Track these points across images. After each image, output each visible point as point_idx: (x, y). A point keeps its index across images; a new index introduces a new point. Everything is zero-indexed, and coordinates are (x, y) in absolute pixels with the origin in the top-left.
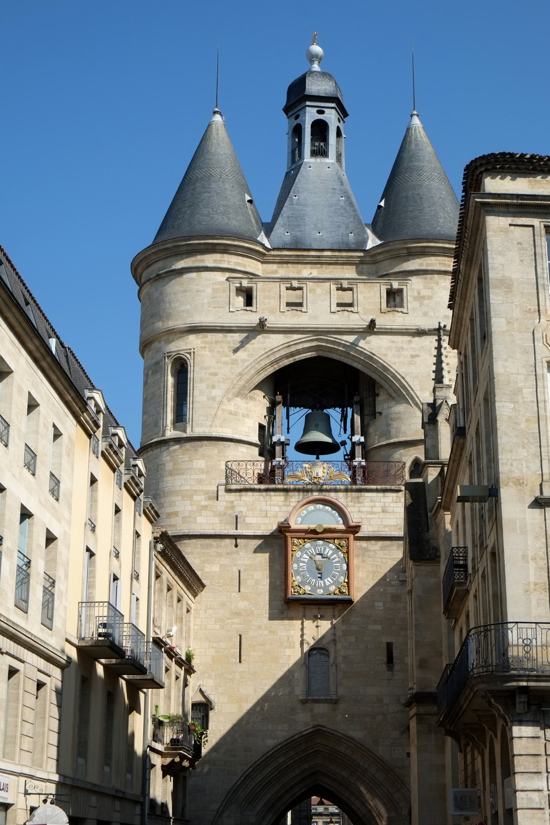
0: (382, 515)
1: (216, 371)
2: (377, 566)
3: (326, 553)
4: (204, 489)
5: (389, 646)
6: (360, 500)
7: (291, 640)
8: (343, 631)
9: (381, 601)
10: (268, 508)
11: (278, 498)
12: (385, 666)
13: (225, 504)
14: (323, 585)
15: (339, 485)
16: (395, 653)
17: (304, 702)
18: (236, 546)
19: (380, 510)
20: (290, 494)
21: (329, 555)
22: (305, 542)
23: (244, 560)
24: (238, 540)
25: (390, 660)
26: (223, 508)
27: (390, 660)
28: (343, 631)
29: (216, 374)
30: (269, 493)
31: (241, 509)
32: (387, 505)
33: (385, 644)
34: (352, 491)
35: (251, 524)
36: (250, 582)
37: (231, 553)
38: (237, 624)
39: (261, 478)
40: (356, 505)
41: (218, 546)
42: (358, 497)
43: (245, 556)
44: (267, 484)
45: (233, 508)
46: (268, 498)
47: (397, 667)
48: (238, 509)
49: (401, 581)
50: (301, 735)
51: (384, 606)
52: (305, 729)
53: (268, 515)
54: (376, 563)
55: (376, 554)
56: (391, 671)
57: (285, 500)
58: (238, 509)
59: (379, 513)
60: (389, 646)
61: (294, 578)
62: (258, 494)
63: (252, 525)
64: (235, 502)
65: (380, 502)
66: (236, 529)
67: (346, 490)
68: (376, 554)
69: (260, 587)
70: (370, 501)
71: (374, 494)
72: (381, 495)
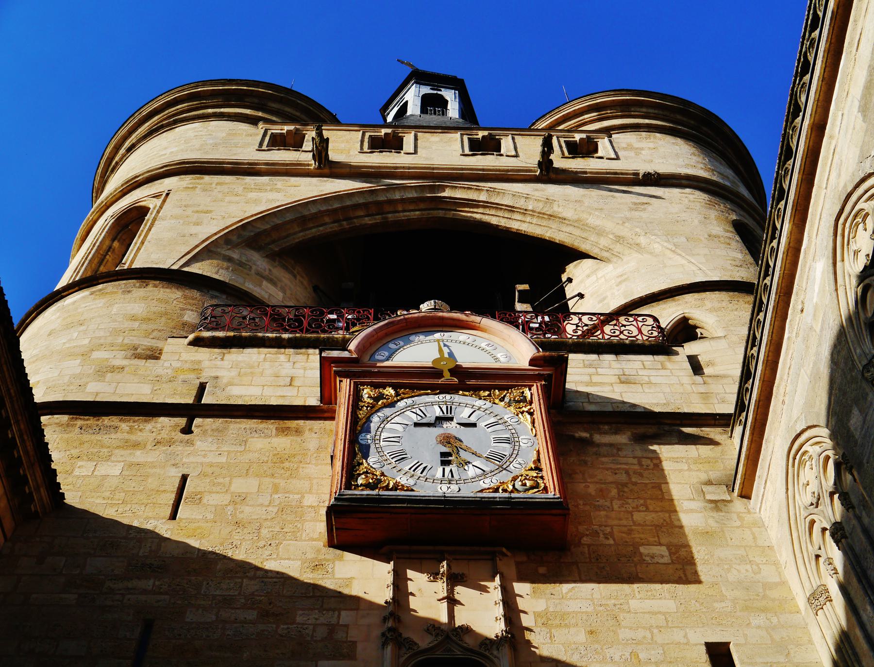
1: (209, 208)
4: (126, 341)
7: (340, 635)
9: (660, 544)
13: (176, 364)
18: (187, 430)
21: (473, 419)
26: (169, 371)
29: (207, 212)
33: (703, 649)
37: (170, 443)
38: (145, 592)
41: (131, 430)
45: (197, 371)
49: (711, 501)
51: (670, 554)
68: (619, 449)
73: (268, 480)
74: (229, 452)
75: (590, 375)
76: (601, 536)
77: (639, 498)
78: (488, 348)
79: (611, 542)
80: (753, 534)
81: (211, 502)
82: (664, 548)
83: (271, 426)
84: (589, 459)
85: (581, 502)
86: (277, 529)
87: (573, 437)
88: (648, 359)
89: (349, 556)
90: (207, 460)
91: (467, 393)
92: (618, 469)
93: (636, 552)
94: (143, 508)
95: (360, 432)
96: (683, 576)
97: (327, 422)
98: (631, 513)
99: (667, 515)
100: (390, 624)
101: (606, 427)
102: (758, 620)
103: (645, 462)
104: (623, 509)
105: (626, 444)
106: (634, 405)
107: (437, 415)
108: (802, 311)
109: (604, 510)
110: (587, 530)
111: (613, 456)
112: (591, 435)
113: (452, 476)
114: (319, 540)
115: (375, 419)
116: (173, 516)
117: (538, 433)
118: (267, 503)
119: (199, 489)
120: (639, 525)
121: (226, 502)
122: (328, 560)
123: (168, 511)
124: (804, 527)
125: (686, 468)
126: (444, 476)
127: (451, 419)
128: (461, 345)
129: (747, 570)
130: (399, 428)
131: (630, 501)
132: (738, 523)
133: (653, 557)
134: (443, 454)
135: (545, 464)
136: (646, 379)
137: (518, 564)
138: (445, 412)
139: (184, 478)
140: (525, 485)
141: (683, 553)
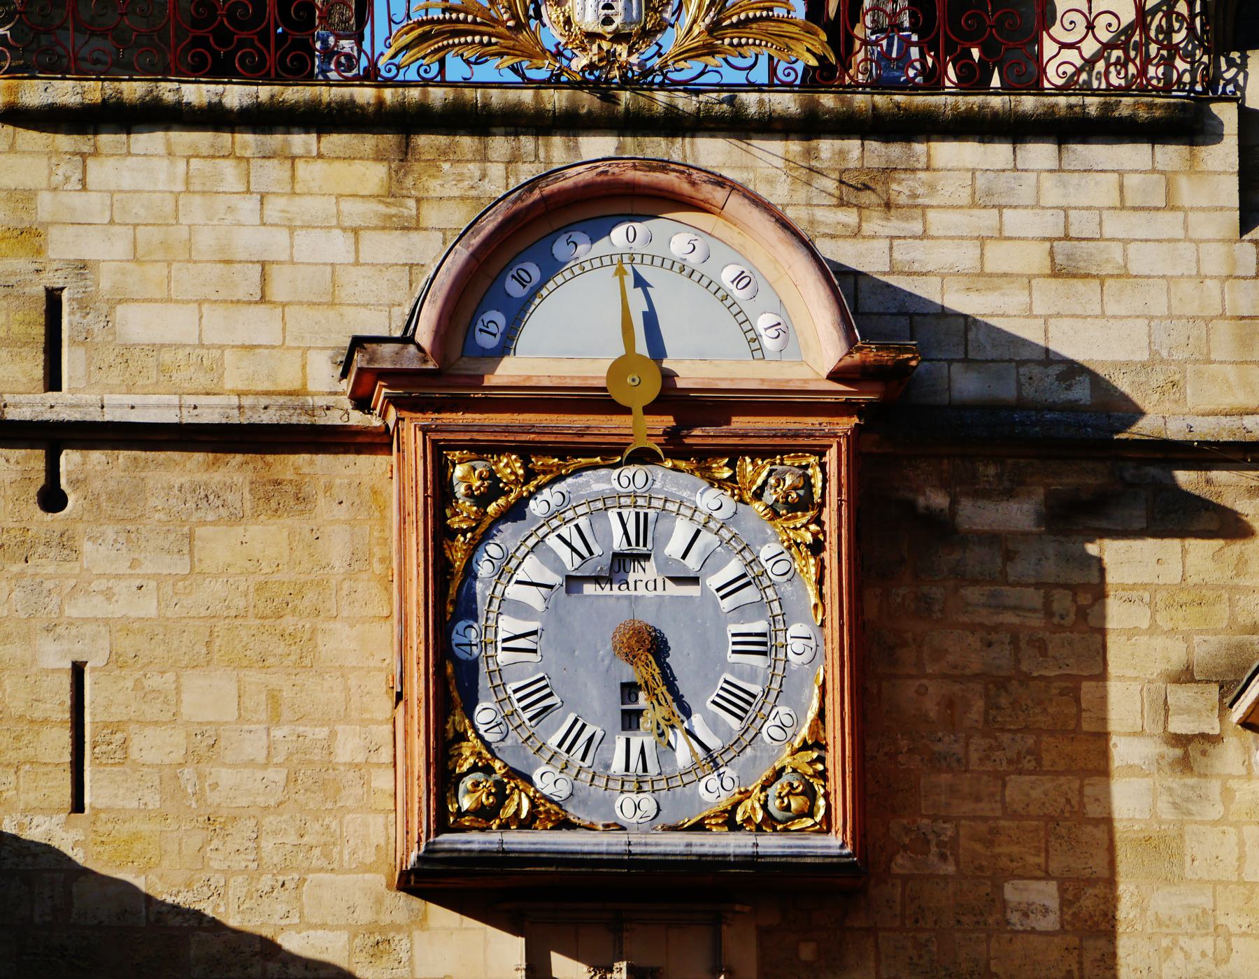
2: (1015, 641)
3: (674, 548)
6: (900, 189)
9: (1048, 876)
10: (276, 243)
11: (344, 171)
15: (758, 88)
18: (52, 499)
19: (1034, 258)
20: (423, 140)
21: (692, 563)
22: (530, 475)
23: (108, 595)
24: (69, 460)
30: (275, 140)
31: (91, 247)
32: (1082, 224)
34: (848, 126)
35: (156, 348)
36: (155, 746)
39: (224, 38)
40: (875, 224)
42: (888, 172)
43: (123, 567)
44: (268, 80)
45: (29, 236)
46: (271, 174)
48: (63, 246)
49: (1180, 740)
51: (1064, 903)
53: (278, 291)
54: (1010, 618)
57: (392, 193)
58: (63, 246)
61: (457, 719)
62: (202, 139)
63: (167, 357)
64: (45, 199)
65: (1037, 206)
66: (53, 381)
67: (807, 127)
68: (1009, 556)
69: (225, 776)
70: (964, 197)
71: (999, 152)
72: (1040, 154)
73: (253, 677)
74: (157, 577)
75: (982, 240)
76: (934, 849)
77: (1026, 729)
78: (738, 294)
79: (950, 869)
80: (1241, 843)
81: (149, 757)
82: (1052, 887)
83: (238, 478)
84: (937, 592)
85: (904, 744)
86: (292, 838)
87: (912, 505)
88: (1132, 155)
89: (441, 916)
90: (116, 610)
91: (683, 464)
92: (995, 628)
93: (996, 902)
94: (12, 778)
95: (456, 618)
96: (1075, 967)
97: (364, 461)
98: (1001, 778)
99: (1076, 785)
101: (992, 471)
103: (1062, 601)
104: (989, 766)
105: (1026, 534)
106: (1073, 370)
107: (616, 548)
109: (950, 769)
110: (908, 831)
111: (993, 581)
112: (954, 502)
113: (645, 769)
114: (376, 871)
115: (484, 569)
116: (78, 805)
117: (828, 623)
118: (261, 757)
119: (118, 713)
120: (1015, 816)
121: (177, 756)
122: (398, 928)
123: (67, 790)
125: (1145, 624)
126: (627, 769)
127: (647, 557)
128: (674, 275)
129: (1204, 954)
130: (534, 598)
131: (1005, 738)
132: (1215, 812)
133: (1026, 915)
134: (629, 690)
135: (832, 733)
136: (1116, 251)
138: (633, 542)
139: (78, 670)
140: (788, 808)
141: (1087, 903)
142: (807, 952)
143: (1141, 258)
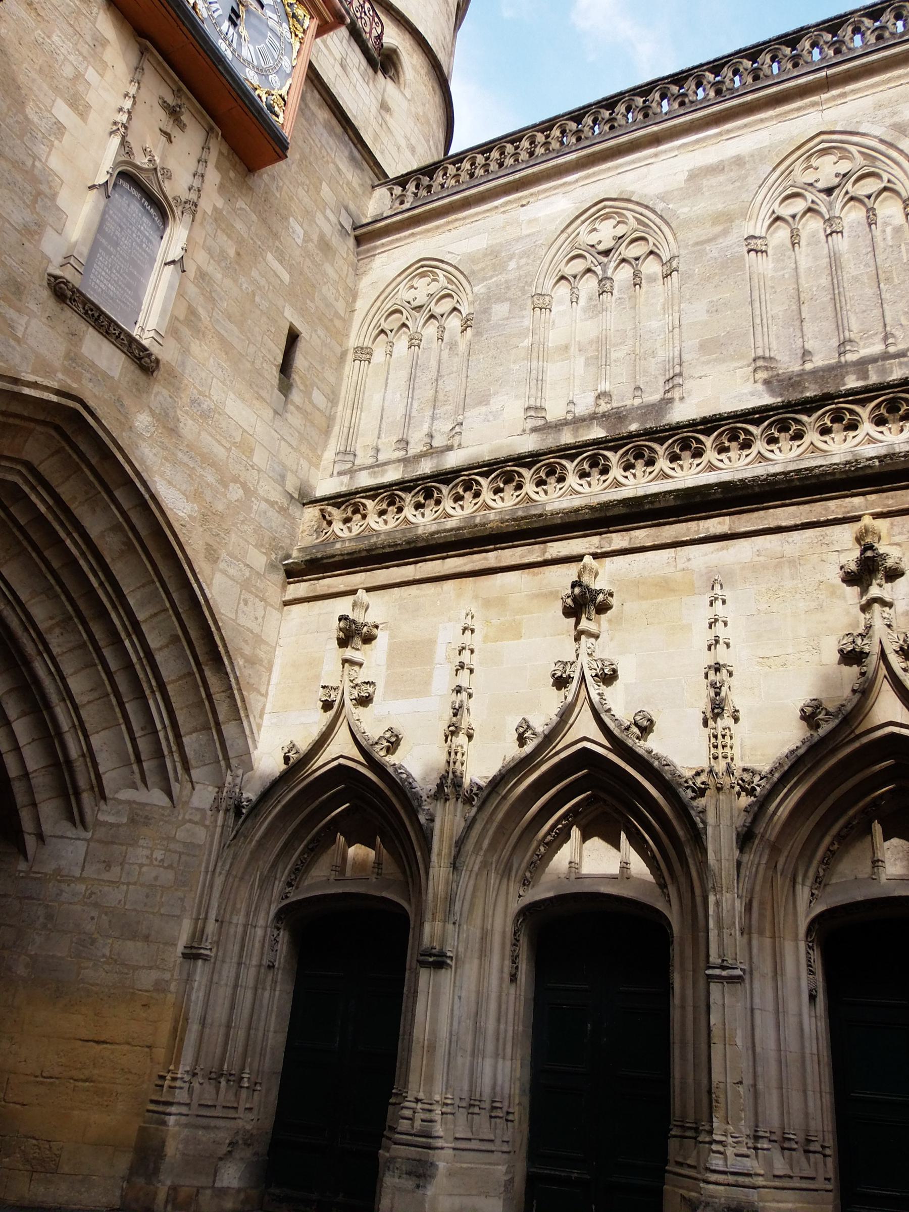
0: (338, 68)
5: (293, 338)
8: (215, 208)
12: (275, 372)
14: (234, 44)
16: (300, 361)
17: (62, 292)
25: (286, 368)
27: (286, 368)
28: (215, 208)
47: (296, 396)
50: (16, 388)
52: (32, 378)
55: (315, 124)
56: (286, 396)
59: (335, 59)
60: (293, 338)
100: (123, 118)
102: (321, 332)
108: (523, 206)
124: (389, 306)
137: (221, 153)
142: (232, 174)
143: (358, 87)
